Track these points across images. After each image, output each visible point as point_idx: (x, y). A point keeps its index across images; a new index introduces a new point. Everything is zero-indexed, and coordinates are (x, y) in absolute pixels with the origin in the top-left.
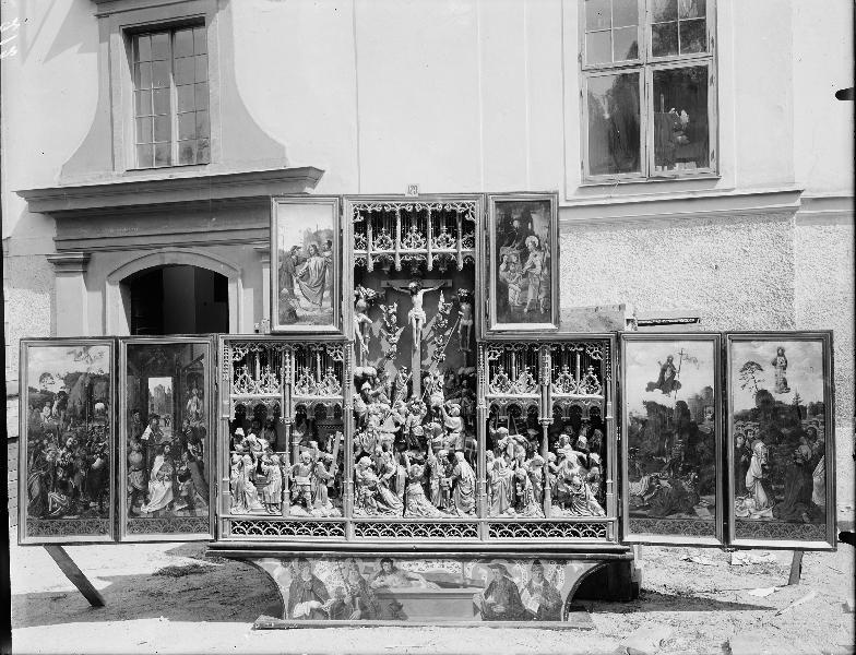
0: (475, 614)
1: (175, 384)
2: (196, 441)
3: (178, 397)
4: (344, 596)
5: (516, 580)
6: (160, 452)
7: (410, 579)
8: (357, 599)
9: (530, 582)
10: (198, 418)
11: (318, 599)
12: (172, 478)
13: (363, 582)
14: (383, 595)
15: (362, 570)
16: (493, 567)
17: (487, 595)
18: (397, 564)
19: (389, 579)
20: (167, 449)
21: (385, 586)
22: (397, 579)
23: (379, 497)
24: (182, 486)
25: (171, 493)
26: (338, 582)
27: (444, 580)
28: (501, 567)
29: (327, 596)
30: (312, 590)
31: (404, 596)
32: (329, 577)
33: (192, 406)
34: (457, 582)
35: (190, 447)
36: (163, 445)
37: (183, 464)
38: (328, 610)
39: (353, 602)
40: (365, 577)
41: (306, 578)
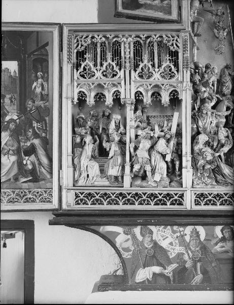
1: (22, 68)
2: (41, 120)
3: (24, 81)
6: (6, 129)
8: (199, 265)
10: (42, 99)
12: (18, 152)
13: (204, 248)
20: (12, 126)
23: (217, 171)
24: (28, 161)
25: (16, 165)
26: (178, 249)
29: (170, 262)
30: (154, 256)
32: (171, 244)
33: (37, 87)
35: (35, 124)
36: (9, 122)
37: (28, 139)
38: (170, 275)
39: (195, 266)
41: (148, 245)
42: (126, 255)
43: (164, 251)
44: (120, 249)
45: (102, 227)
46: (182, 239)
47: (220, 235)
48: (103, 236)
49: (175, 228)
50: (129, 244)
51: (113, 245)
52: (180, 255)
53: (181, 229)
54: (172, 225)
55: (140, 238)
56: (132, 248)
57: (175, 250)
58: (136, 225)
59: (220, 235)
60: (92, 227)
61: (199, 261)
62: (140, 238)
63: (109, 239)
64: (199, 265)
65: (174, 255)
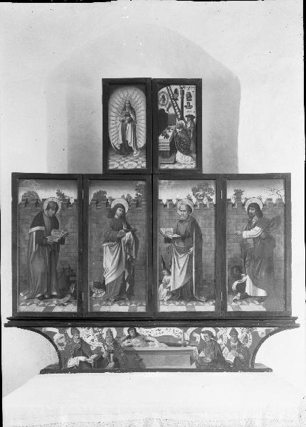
0: (191, 364)
5: (219, 341)
7: (149, 341)
8: (112, 355)
11: (84, 355)
13: (115, 343)
14: (130, 351)
18: (138, 330)
19: (133, 341)
21: (131, 346)
22: (139, 341)
27: (171, 341)
28: (210, 334)
29: (91, 353)
32: (93, 340)
34: (180, 342)
38: (92, 362)
42: (60, 348)
43: (88, 346)
44: (56, 344)
45: (44, 328)
46: (100, 338)
47: (127, 334)
48: (45, 335)
49: (96, 329)
50: (63, 341)
51: (51, 341)
52: (98, 349)
53: (100, 330)
54: (93, 327)
55: (71, 336)
56: (65, 344)
57: (95, 345)
58: (69, 326)
59: (127, 334)
60: (36, 328)
61: (113, 353)
62: (71, 336)
63: (49, 337)
64: (112, 355)
65: (94, 348)
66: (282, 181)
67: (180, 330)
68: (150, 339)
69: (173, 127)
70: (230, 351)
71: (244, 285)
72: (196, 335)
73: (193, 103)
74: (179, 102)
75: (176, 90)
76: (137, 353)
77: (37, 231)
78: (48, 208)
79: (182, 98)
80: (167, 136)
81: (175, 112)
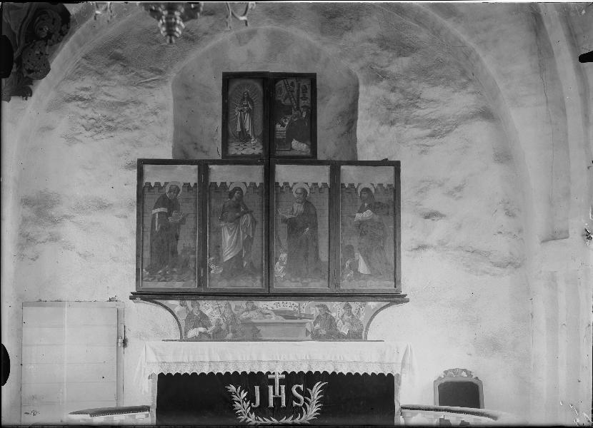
0: (307, 335)
4: (221, 325)
5: (334, 315)
9: (343, 316)
11: (204, 326)
14: (247, 323)
15: (233, 307)
16: (318, 306)
17: (315, 323)
19: (252, 314)
26: (217, 316)
28: (324, 306)
29: (210, 325)
31: (260, 324)
38: (211, 334)
39: (227, 328)
40: (236, 313)
47: (245, 307)
48: (166, 308)
55: (191, 309)
59: (245, 307)
62: (191, 309)
66: (392, 168)
67: (296, 303)
68: (268, 312)
69: (289, 117)
70: (344, 323)
71: (357, 263)
72: (312, 308)
73: (308, 95)
74: (295, 94)
75: (292, 84)
76: (254, 324)
77: (160, 213)
78: (170, 191)
79: (298, 90)
80: (283, 125)
81: (291, 101)
